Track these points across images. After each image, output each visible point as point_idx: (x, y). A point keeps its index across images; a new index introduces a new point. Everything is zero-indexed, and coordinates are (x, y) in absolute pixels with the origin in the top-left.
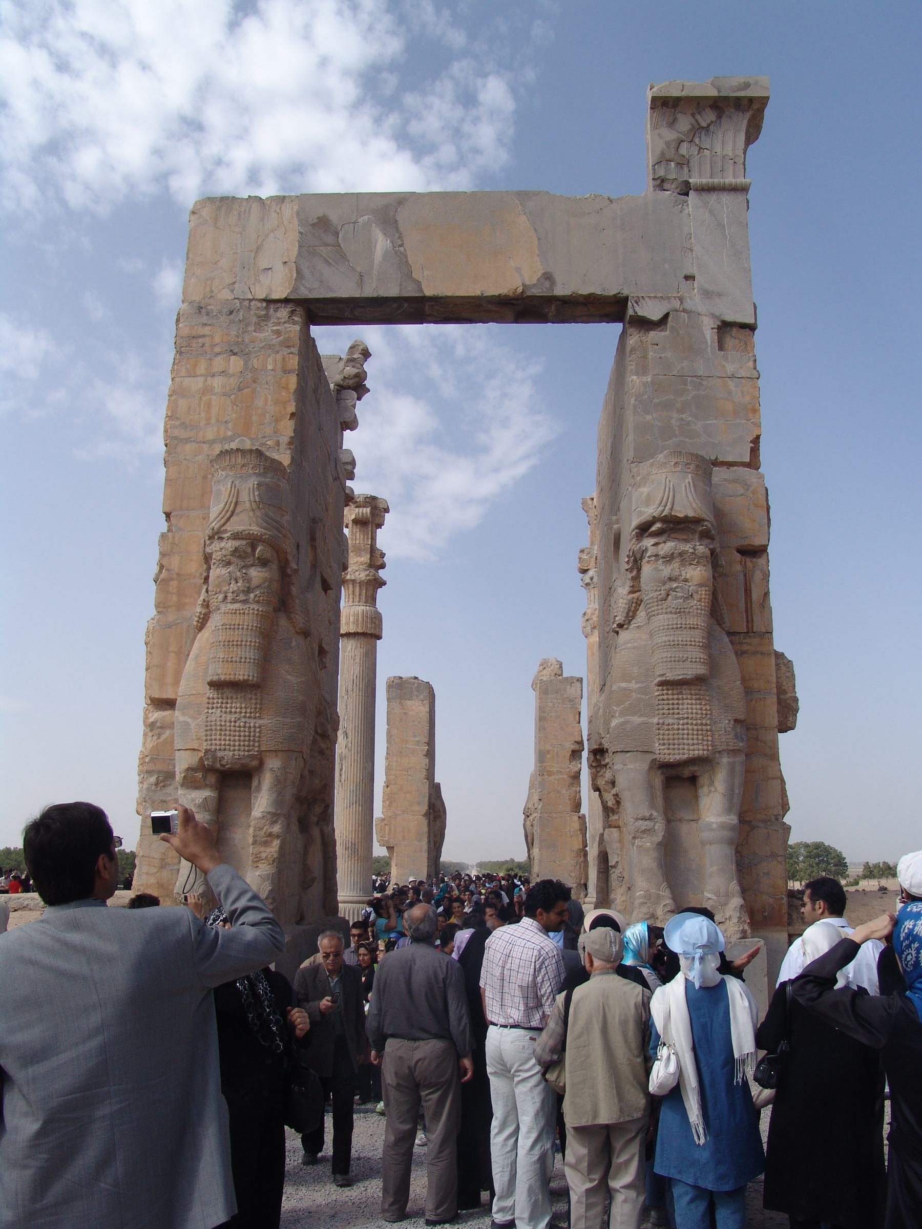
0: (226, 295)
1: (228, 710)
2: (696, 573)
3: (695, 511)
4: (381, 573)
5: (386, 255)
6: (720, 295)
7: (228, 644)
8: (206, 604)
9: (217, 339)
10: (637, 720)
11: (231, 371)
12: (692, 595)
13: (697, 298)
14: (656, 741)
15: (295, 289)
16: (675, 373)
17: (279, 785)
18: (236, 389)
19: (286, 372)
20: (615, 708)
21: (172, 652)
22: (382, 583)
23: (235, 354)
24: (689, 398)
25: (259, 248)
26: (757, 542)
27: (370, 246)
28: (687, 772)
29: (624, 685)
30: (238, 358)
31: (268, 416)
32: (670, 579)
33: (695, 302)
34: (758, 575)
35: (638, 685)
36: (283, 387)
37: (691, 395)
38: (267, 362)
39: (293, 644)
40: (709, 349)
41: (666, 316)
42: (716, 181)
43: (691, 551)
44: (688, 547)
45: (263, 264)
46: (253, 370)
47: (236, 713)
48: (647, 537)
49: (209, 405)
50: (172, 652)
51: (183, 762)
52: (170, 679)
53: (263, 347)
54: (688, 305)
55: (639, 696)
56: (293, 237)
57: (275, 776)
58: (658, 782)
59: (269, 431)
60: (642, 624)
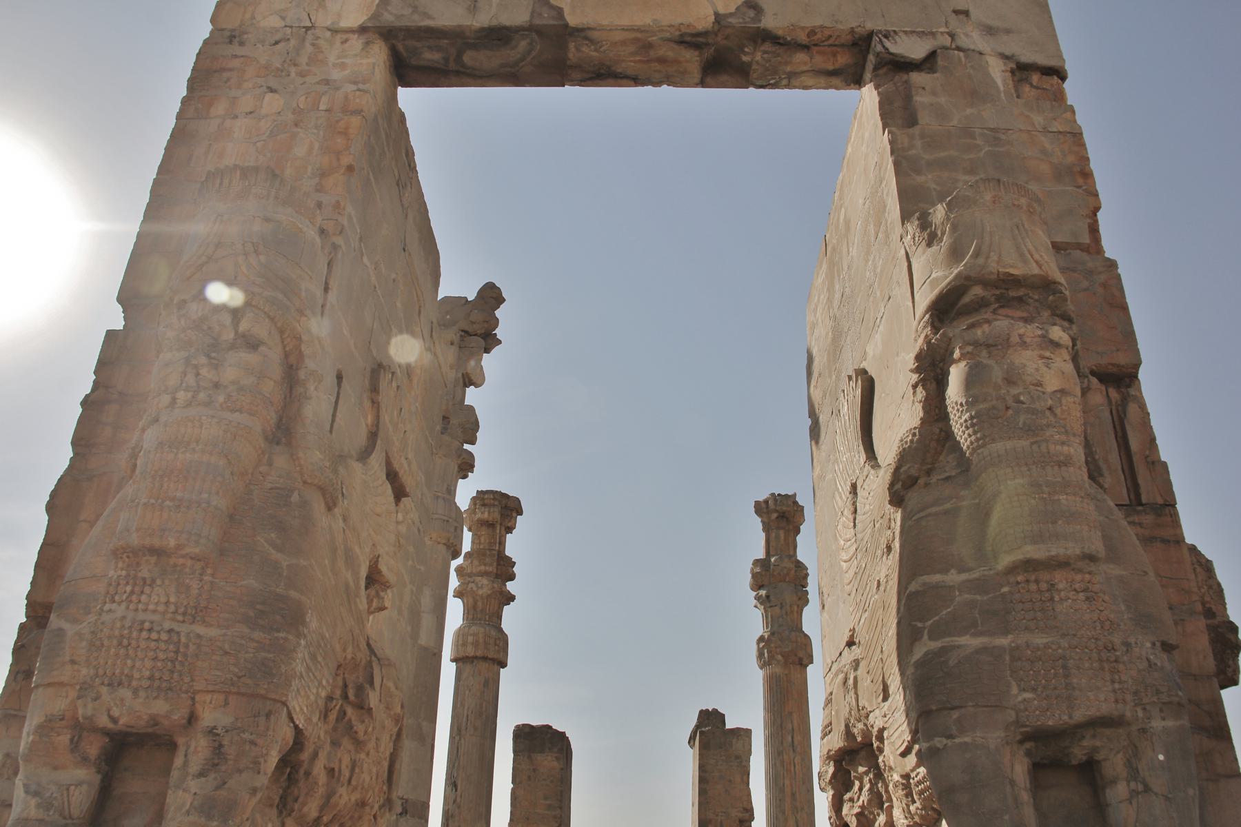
1: (140, 606)
3: (1040, 267)
4: (511, 586)
11: (263, 112)
12: (1050, 409)
14: (1014, 683)
16: (955, 122)
18: (267, 134)
20: (920, 625)
21: (85, 521)
22: (510, 598)
23: (272, 90)
24: (982, 154)
26: (1122, 359)
29: (937, 578)
30: (277, 96)
31: (309, 170)
34: (1132, 408)
35: (964, 576)
36: (339, 133)
37: (984, 151)
38: (319, 102)
39: (293, 499)
40: (1002, 95)
43: (1040, 332)
47: (155, 611)
48: (954, 319)
50: (85, 521)
53: (318, 83)
55: (967, 596)
57: (216, 744)
60: (953, 474)
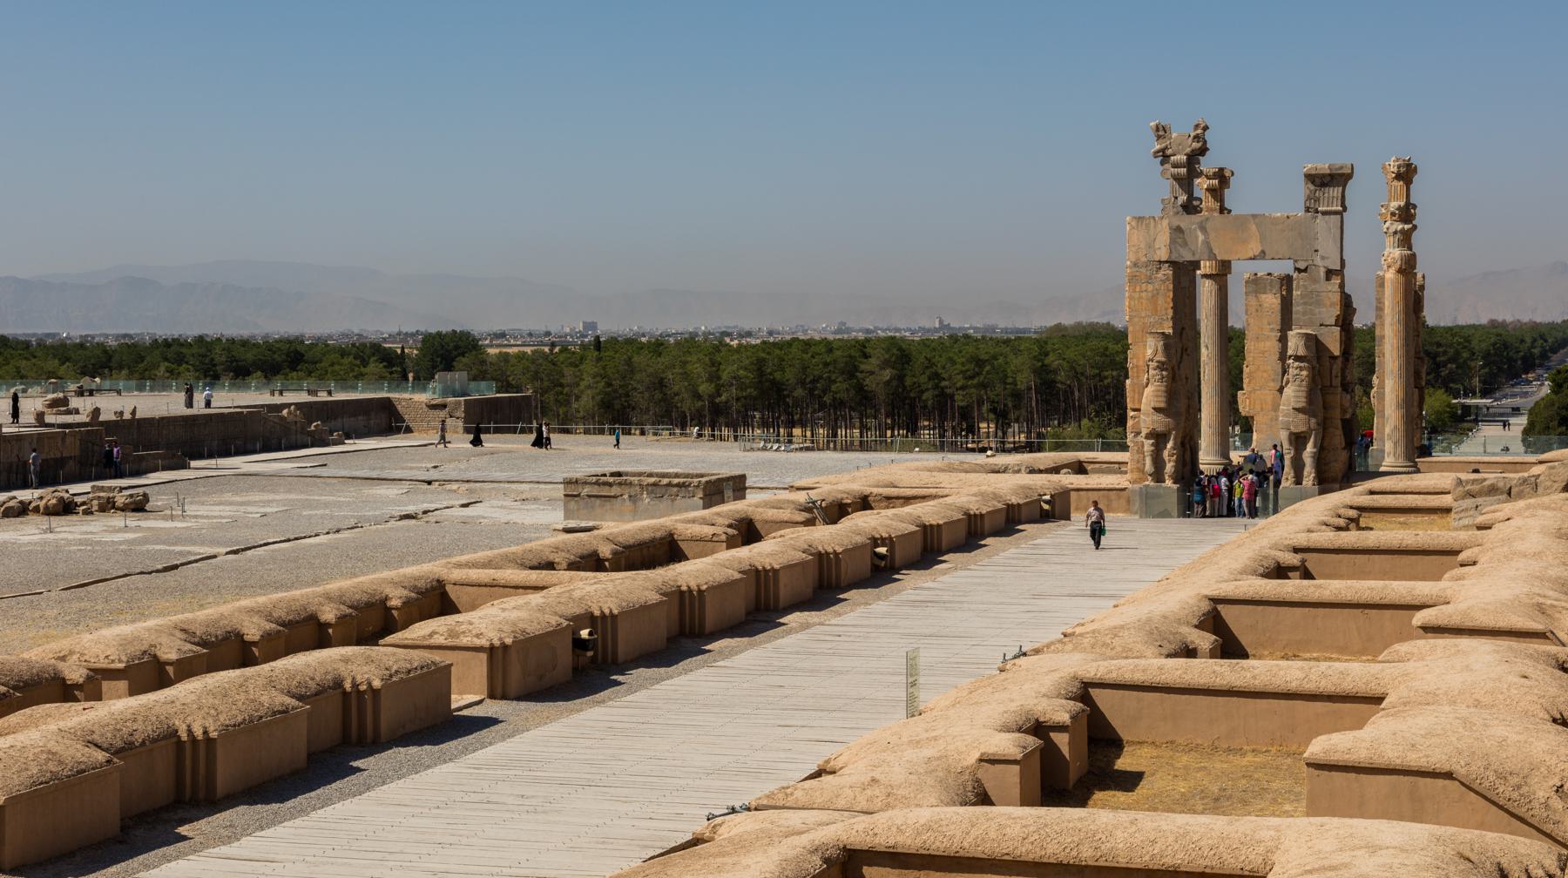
0: (1144, 259)
2: (1305, 373)
5: (1203, 241)
6: (1328, 258)
7: (1157, 396)
8: (1148, 379)
9: (1143, 277)
10: (1286, 419)
13: (1319, 260)
15: (1170, 257)
17: (1175, 439)
19: (1169, 290)
25: (1155, 239)
27: (1197, 238)
28: (1303, 435)
32: (1297, 375)
33: (1318, 261)
41: (1307, 267)
42: (1329, 209)
44: (1302, 365)
45: (1157, 247)
46: (1157, 290)
49: (1142, 303)
51: (1144, 432)
52: (1136, 401)
54: (1315, 263)
56: (1168, 234)
58: (1293, 437)
59: (1164, 312)
